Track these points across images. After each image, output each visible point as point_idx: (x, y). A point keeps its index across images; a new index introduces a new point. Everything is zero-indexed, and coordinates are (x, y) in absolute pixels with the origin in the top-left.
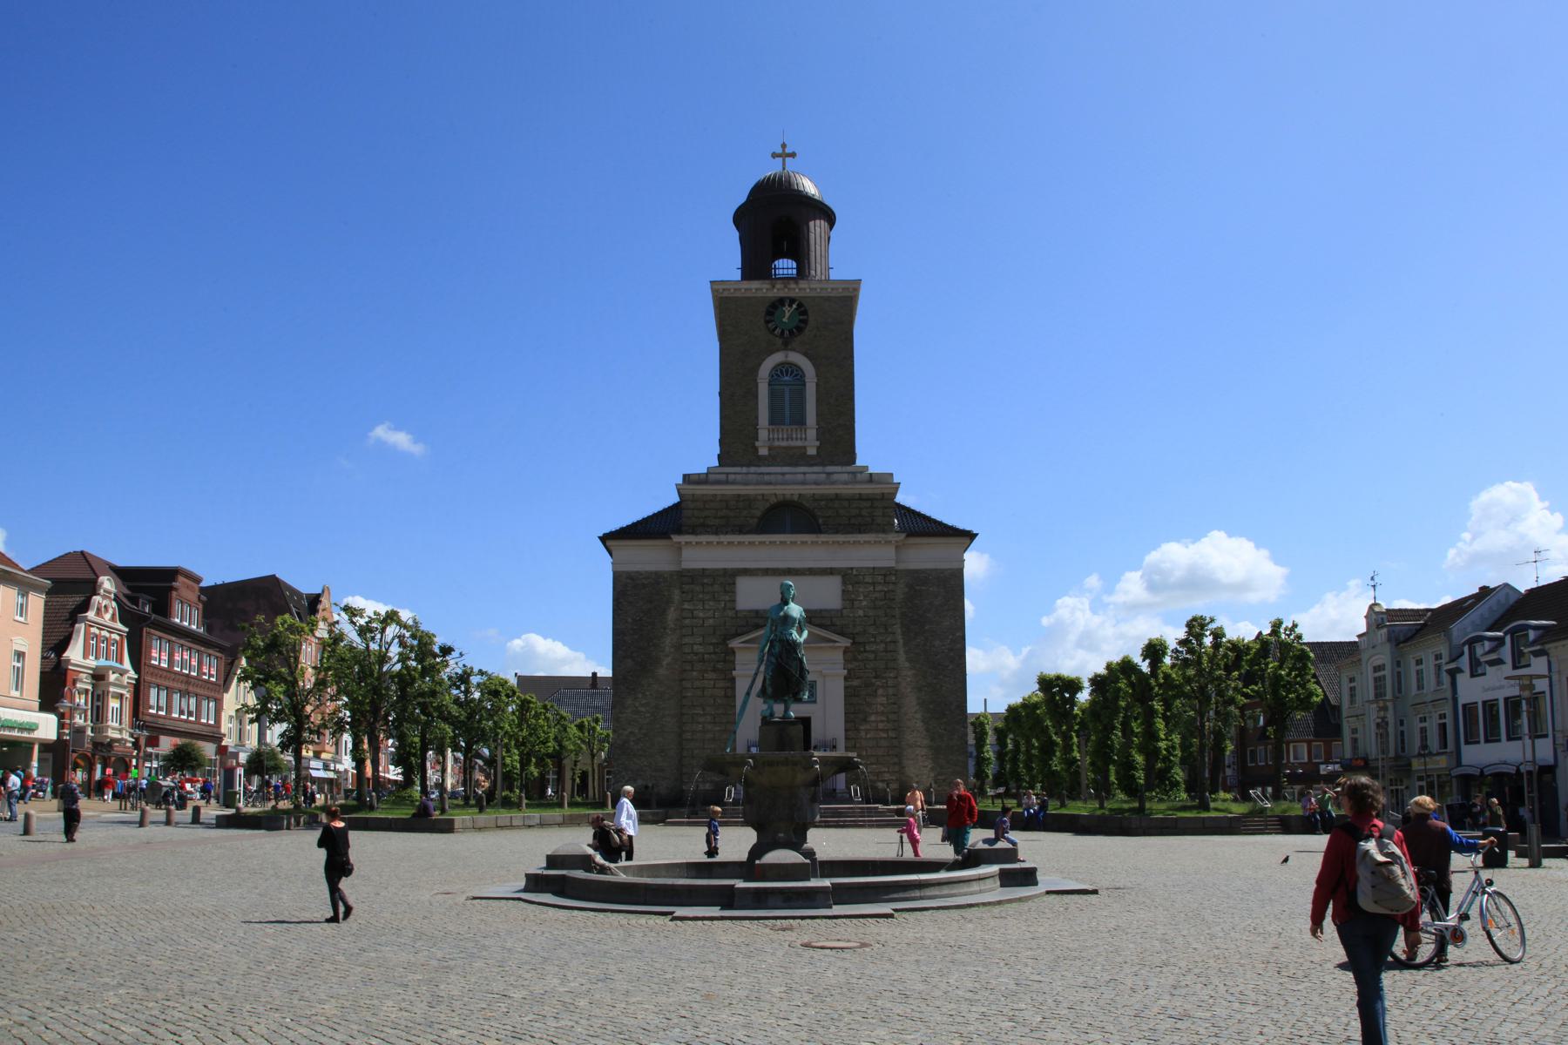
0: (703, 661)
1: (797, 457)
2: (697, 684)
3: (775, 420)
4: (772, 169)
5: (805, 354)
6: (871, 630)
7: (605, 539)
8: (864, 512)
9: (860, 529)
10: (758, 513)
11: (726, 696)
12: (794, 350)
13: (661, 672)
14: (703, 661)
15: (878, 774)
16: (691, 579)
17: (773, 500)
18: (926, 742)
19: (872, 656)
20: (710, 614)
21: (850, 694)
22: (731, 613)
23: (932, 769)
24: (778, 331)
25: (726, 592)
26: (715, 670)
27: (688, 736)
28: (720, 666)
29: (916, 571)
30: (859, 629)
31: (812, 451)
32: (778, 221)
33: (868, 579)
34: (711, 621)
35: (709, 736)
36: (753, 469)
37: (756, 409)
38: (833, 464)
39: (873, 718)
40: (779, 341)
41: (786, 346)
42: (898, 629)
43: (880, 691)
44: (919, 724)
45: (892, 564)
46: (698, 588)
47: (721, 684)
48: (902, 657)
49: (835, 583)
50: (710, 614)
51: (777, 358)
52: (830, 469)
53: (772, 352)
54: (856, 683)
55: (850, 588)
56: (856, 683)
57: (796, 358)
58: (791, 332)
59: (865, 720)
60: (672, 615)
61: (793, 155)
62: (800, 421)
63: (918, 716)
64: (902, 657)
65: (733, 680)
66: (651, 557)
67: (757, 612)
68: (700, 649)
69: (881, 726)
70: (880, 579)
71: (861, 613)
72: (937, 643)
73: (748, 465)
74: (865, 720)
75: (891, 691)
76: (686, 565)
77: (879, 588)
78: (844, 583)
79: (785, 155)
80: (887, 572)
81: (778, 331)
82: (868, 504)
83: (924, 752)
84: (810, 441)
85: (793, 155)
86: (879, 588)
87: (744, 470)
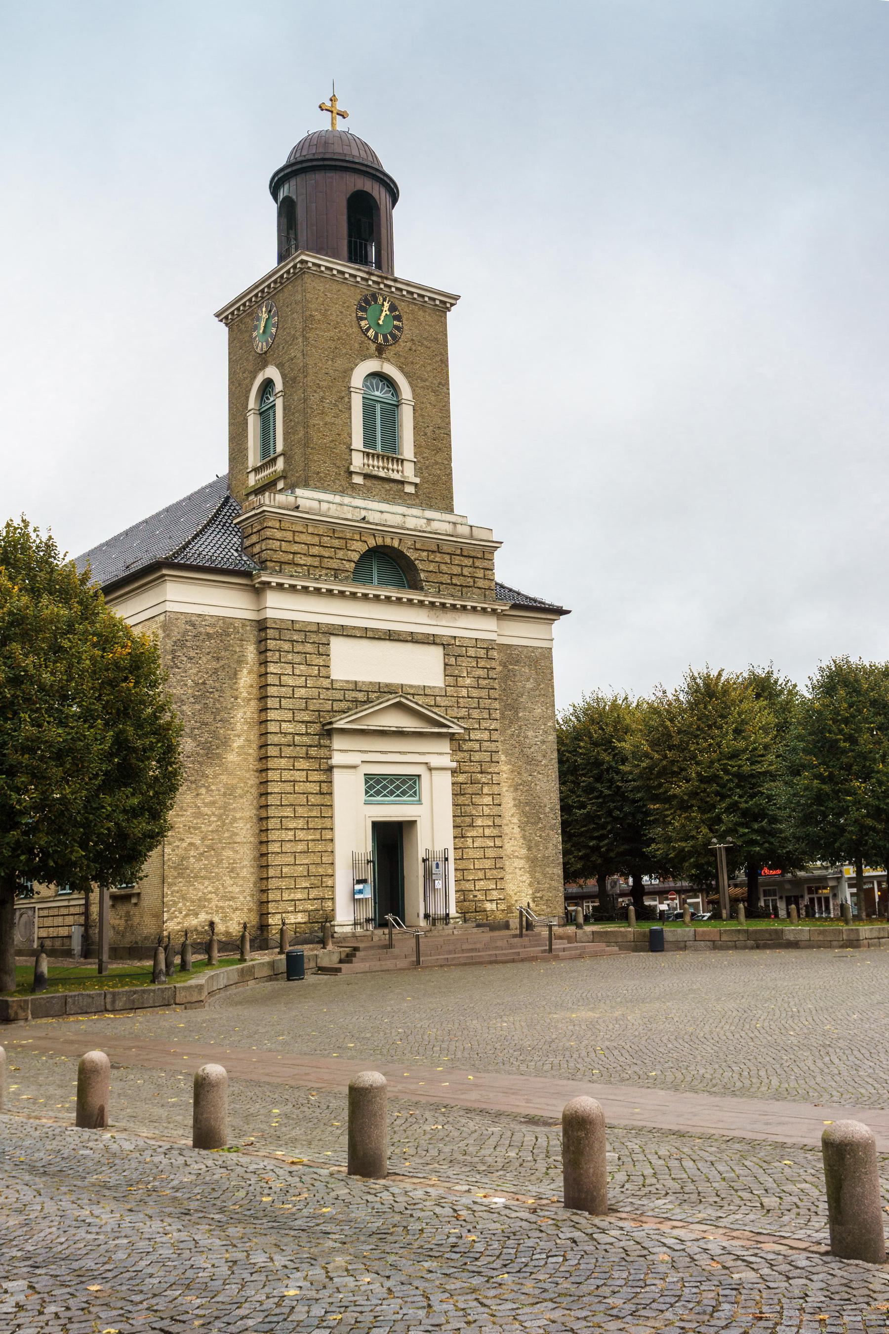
2: (286, 775)
3: (369, 439)
4: (322, 123)
5: (401, 369)
6: (475, 714)
8: (466, 571)
10: (356, 557)
13: (232, 757)
17: (372, 543)
18: (524, 851)
19: (476, 746)
20: (301, 681)
21: (458, 791)
22: (326, 683)
23: (530, 885)
24: (371, 333)
26: (308, 757)
27: (274, 848)
28: (313, 752)
29: (509, 646)
30: (463, 712)
31: (409, 489)
32: (336, 200)
33: (471, 652)
34: (302, 692)
35: (301, 847)
36: (347, 500)
37: (348, 424)
38: (430, 507)
40: (373, 347)
41: (380, 351)
44: (517, 830)
46: (287, 646)
47: (315, 776)
49: (434, 656)
50: (301, 681)
52: (429, 514)
53: (365, 358)
54: (461, 778)
55: (452, 660)
56: (461, 778)
57: (390, 370)
58: (385, 339)
59: (471, 825)
61: (343, 115)
63: (515, 820)
65: (330, 769)
68: (287, 727)
69: (487, 832)
70: (482, 653)
71: (464, 692)
72: (530, 733)
73: (342, 492)
74: (471, 825)
76: (270, 614)
79: (330, 108)
81: (371, 333)
82: (468, 562)
83: (521, 863)
85: (343, 115)
86: (482, 663)
87: (338, 499)
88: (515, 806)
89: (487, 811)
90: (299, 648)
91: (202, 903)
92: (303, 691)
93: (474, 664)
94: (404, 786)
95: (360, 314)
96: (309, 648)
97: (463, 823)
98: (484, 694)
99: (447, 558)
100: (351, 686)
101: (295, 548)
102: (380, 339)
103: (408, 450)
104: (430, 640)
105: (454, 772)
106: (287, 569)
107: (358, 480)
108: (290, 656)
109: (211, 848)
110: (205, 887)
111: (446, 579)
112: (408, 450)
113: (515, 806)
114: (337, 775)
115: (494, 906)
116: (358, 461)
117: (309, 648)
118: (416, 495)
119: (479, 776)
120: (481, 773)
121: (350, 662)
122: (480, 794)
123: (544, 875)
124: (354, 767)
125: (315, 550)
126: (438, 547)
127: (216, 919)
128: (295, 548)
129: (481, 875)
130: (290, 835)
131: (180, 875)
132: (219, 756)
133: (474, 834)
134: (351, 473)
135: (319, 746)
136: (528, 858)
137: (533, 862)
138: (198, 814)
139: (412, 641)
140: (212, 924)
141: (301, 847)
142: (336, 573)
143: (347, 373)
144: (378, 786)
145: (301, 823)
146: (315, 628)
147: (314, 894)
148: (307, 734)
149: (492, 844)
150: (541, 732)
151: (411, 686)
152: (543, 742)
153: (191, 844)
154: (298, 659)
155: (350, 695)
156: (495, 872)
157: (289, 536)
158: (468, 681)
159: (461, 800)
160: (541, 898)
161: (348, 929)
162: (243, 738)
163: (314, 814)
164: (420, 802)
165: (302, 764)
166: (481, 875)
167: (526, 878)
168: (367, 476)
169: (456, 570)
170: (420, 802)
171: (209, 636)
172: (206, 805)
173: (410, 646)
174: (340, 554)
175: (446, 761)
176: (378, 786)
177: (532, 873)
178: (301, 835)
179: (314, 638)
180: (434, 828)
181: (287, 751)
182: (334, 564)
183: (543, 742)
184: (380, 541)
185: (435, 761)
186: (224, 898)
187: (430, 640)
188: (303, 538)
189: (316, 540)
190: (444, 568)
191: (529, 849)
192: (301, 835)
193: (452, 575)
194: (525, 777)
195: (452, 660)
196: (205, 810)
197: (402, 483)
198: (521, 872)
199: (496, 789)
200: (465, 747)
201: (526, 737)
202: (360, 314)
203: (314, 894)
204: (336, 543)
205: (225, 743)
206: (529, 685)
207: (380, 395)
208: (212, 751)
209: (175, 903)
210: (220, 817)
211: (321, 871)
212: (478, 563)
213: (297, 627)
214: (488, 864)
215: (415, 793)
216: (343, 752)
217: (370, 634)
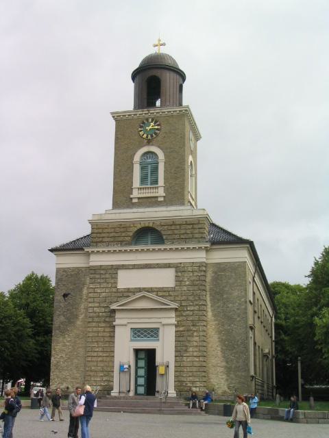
0: (98, 317)
1: (151, 202)
5: (159, 147)
6: (191, 298)
7: (52, 250)
8: (188, 232)
9: (186, 240)
10: (131, 234)
11: (110, 336)
12: (152, 145)
13: (79, 323)
14: (98, 317)
15: (193, 382)
16: (94, 270)
17: (139, 227)
18: (224, 364)
19: (191, 313)
21: (179, 335)
22: (114, 290)
23: (227, 380)
24: (145, 136)
25: (112, 278)
26: (105, 322)
28: (107, 320)
31: (162, 199)
32: (155, 80)
33: (190, 269)
34: (104, 294)
35: (100, 359)
37: (131, 178)
39: (191, 349)
41: (149, 142)
42: (208, 298)
43: (195, 334)
44: (219, 353)
45: (204, 260)
46: (97, 276)
48: (210, 314)
51: (145, 149)
53: (141, 146)
54: (181, 329)
55: (180, 274)
58: (152, 136)
59: (186, 351)
60: (85, 291)
62: (155, 182)
63: (219, 349)
64: (210, 314)
65: (114, 326)
66: (73, 261)
67: (129, 289)
69: (195, 354)
71: (185, 288)
74: (186, 351)
75: (201, 334)
76: (91, 264)
77: (196, 274)
78: (176, 272)
80: (201, 265)
84: (161, 192)
86: (196, 274)
88: (219, 341)
89: (195, 344)
90: (103, 276)
91: (64, 380)
92: (104, 294)
93: (191, 274)
94: (153, 333)
95: (140, 129)
96: (107, 276)
97: (180, 351)
98: (196, 288)
99: (178, 227)
100: (126, 290)
101: (103, 235)
102: (149, 136)
103: (161, 181)
104: (168, 266)
105: (176, 326)
106: (99, 244)
107: (134, 201)
108: (99, 280)
109: (69, 358)
110: (66, 373)
111: (177, 237)
112: (161, 181)
113: (219, 341)
114: (117, 328)
115: (198, 389)
116: (135, 194)
117: (107, 276)
118: (165, 201)
119: (192, 327)
120: (193, 326)
121: (126, 280)
122: (192, 336)
123: (236, 376)
124: (126, 325)
125: (112, 235)
126: (173, 224)
127: (70, 387)
128: (103, 235)
129: (190, 374)
130: (95, 354)
131: (57, 368)
132: (73, 322)
133: (188, 355)
134: (131, 199)
135: (110, 317)
136: (226, 367)
137: (228, 370)
138: (65, 345)
139: (158, 267)
140: (68, 388)
141: (100, 359)
142: (122, 243)
143: (132, 157)
144: (138, 333)
145: (100, 349)
146: (110, 267)
147: (105, 379)
148: (105, 312)
149: (197, 360)
150: (237, 304)
151: (156, 288)
152: (238, 309)
153: (61, 356)
154: (102, 281)
155: (126, 294)
156: (198, 373)
157: (100, 231)
158: (187, 283)
159: (181, 339)
160: (233, 387)
161: (117, 395)
162: (83, 315)
163: (107, 345)
164: (158, 340)
165: (103, 325)
166: (190, 374)
167: (224, 376)
168: (139, 198)
169: (183, 232)
170: (158, 340)
171: (71, 275)
172: (68, 342)
173: (157, 270)
174: (123, 234)
175: (173, 321)
176: (138, 333)
177: (228, 373)
178: (101, 354)
179: (110, 271)
180: (166, 353)
181: (96, 319)
182: (121, 239)
183: (238, 309)
184: (143, 226)
185: (165, 321)
186: (73, 378)
187: (168, 266)
188: (106, 231)
189: (113, 230)
190: (176, 232)
191: (227, 362)
192: (101, 354)
193: (180, 234)
194: (227, 327)
195: (180, 274)
196: (68, 344)
197: (157, 197)
198: (222, 374)
199: (201, 334)
200: (184, 314)
201: (228, 307)
202: (140, 129)
203: (105, 379)
204: (122, 230)
205: (76, 317)
206: (231, 281)
207: (150, 160)
208: (71, 319)
209: (54, 379)
210: (73, 347)
211: (109, 369)
212: (195, 226)
213: (103, 268)
214: (195, 369)
215: (158, 336)
216: (120, 319)
217: (136, 267)
